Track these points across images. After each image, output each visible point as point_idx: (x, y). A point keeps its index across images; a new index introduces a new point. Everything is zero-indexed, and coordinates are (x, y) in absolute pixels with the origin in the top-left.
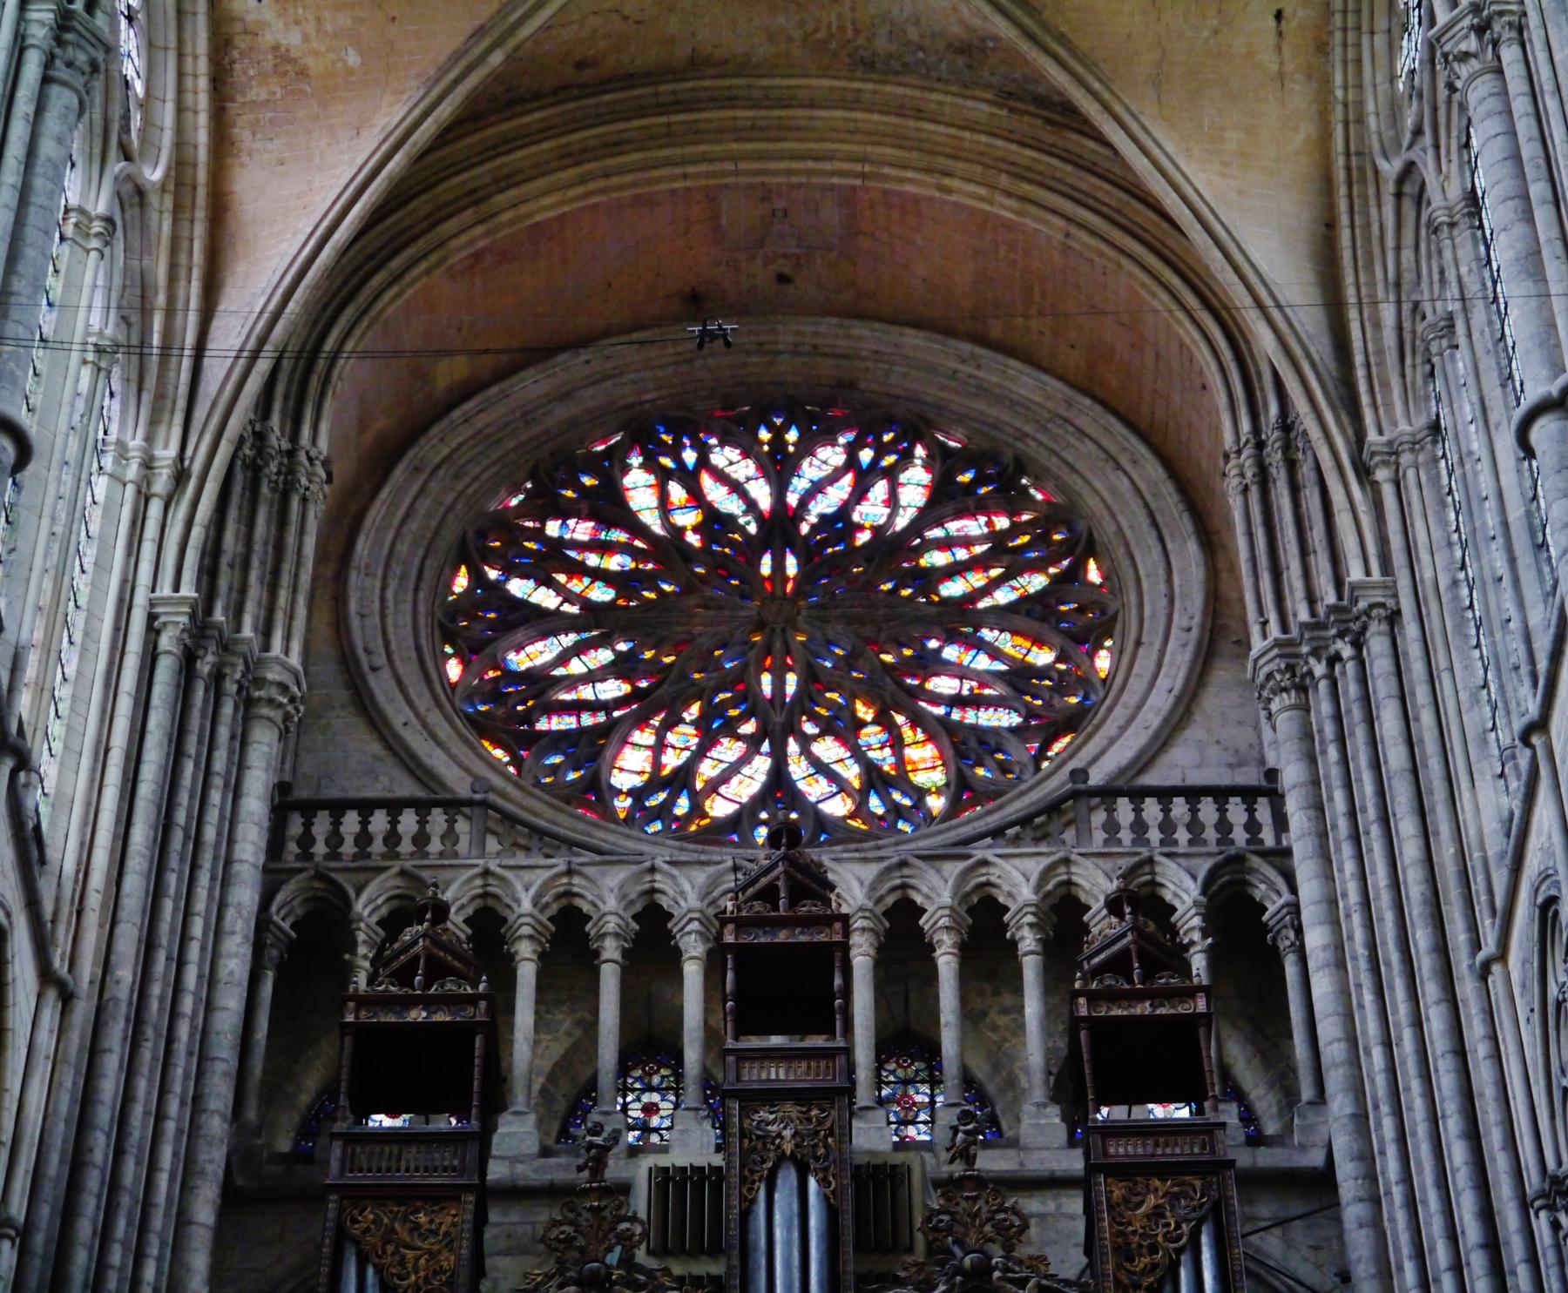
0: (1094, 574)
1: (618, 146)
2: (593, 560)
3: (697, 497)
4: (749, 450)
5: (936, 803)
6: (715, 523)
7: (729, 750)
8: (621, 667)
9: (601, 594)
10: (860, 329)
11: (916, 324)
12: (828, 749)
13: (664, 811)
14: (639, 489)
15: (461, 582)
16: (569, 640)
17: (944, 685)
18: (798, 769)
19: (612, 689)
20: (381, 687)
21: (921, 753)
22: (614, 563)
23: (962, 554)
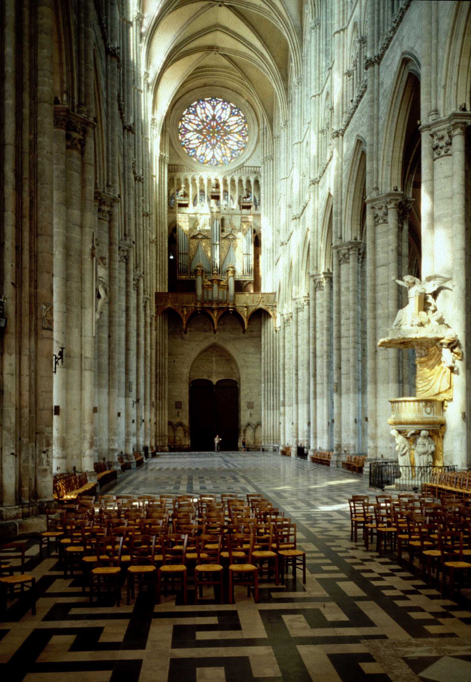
0: (247, 127)
1: (198, 76)
2: (194, 121)
3: (205, 113)
4: (210, 103)
5: (229, 159)
6: (207, 117)
7: (208, 150)
8: (198, 138)
9: (195, 127)
10: (223, 89)
11: (229, 89)
12: (219, 151)
13: (202, 159)
14: (198, 109)
15: (180, 124)
16: (192, 134)
17: (230, 142)
18: (215, 154)
19: (197, 141)
20: (173, 142)
21: (228, 151)
22: (196, 122)
23: (233, 123)
